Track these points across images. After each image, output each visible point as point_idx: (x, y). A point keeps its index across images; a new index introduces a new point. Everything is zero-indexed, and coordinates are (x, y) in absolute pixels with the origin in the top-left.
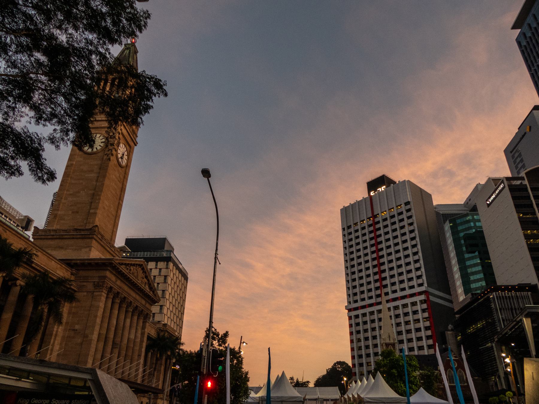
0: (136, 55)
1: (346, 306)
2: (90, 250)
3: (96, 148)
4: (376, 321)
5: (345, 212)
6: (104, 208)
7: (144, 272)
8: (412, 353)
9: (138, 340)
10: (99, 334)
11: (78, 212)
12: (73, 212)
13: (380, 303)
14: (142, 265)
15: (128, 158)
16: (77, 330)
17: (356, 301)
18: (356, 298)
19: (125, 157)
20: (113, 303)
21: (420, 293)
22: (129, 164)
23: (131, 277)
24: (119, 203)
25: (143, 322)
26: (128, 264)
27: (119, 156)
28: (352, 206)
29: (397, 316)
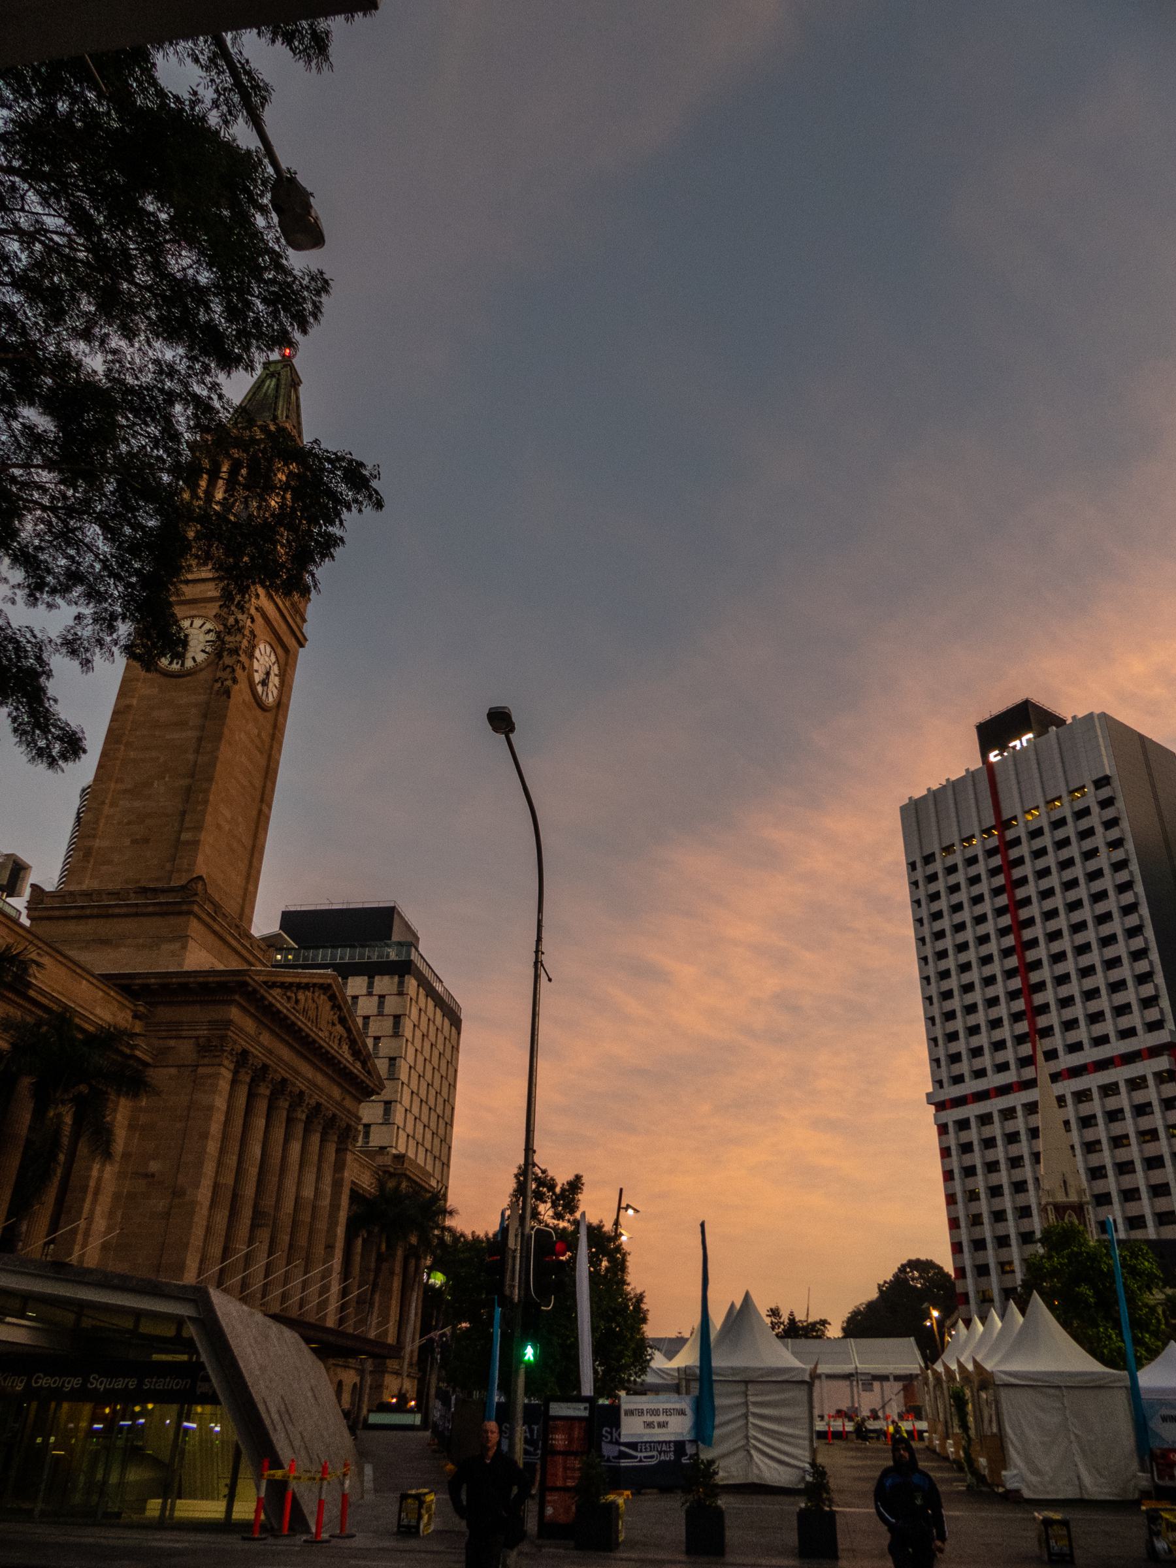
0: (296, 391)
1: (928, 1095)
2: (184, 947)
3: (194, 658)
4: (1023, 1137)
5: (916, 815)
6: (219, 827)
7: (336, 1007)
8: (1138, 1234)
9: (326, 1202)
10: (216, 1186)
11: (146, 841)
12: (134, 842)
13: (1031, 1084)
14: (330, 985)
15: (282, 682)
16: (153, 1175)
17: (958, 1079)
18: (957, 1069)
19: (274, 680)
20: (251, 1096)
21: (1154, 1052)
22: (284, 700)
23: (301, 1022)
24: (260, 811)
25: (338, 1151)
26: (291, 984)
27: (257, 677)
28: (935, 796)
29: (1087, 1122)
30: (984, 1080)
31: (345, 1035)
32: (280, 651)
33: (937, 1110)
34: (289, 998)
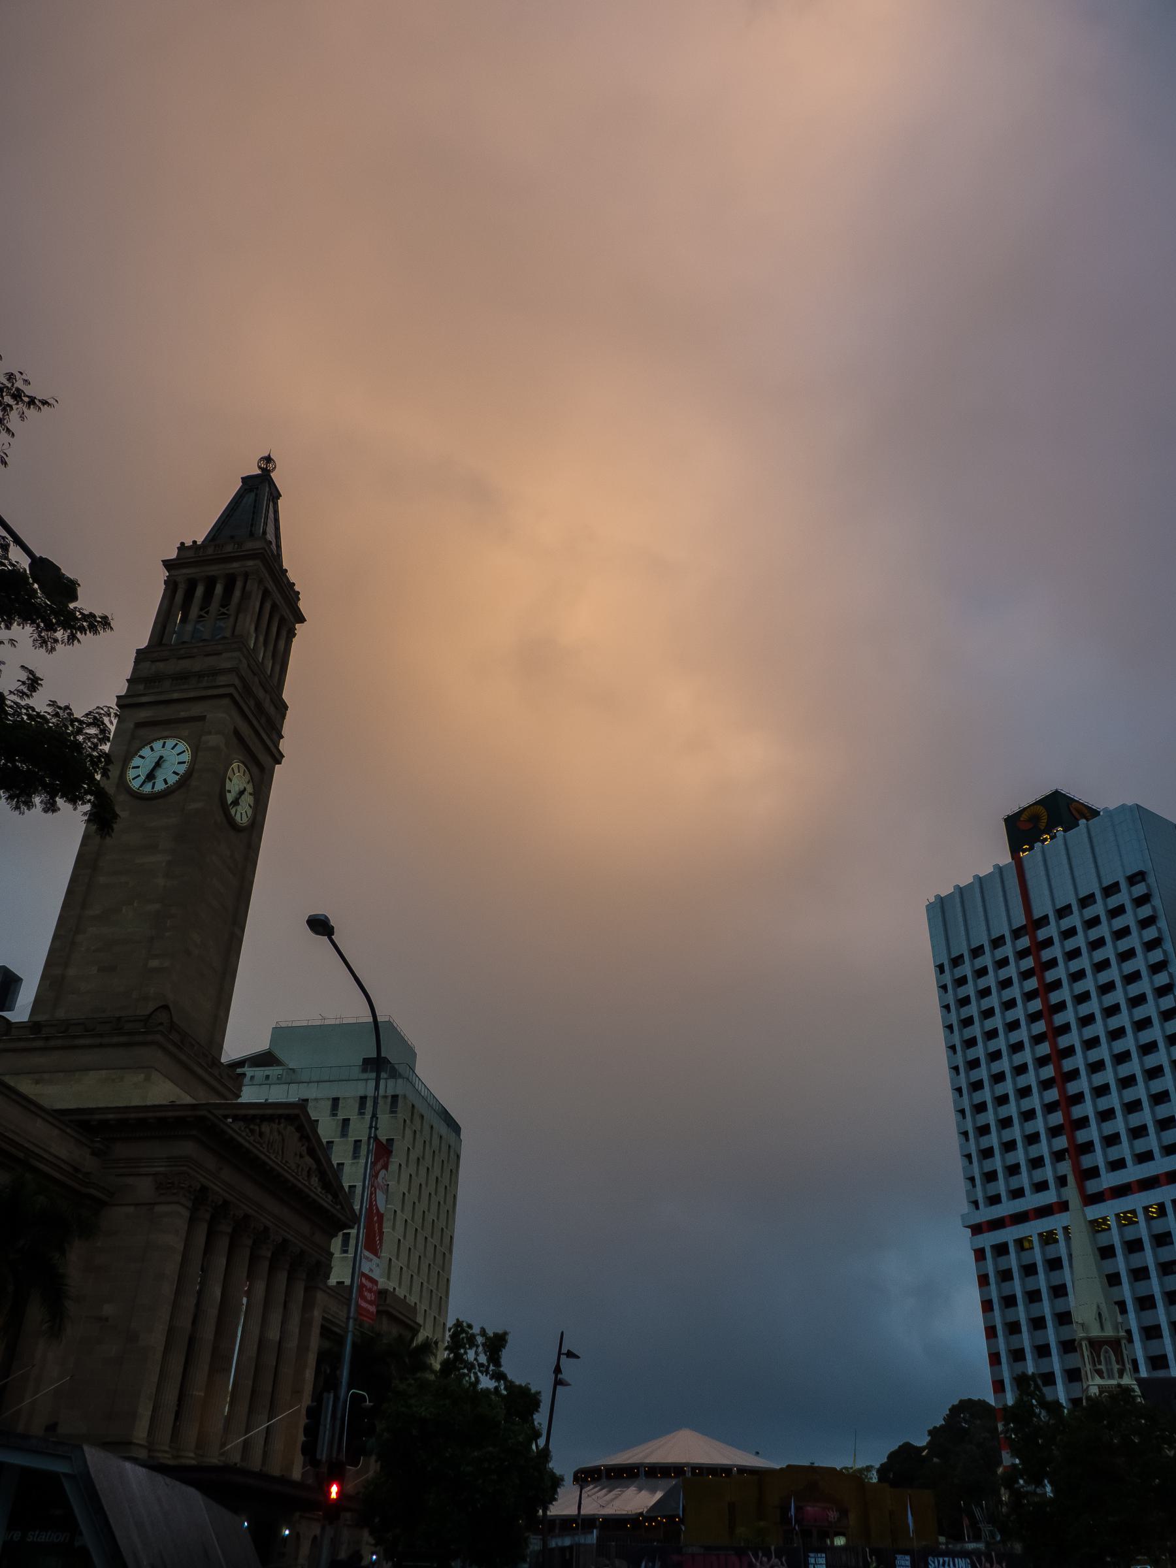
0: (276, 505)
9: (292, 1344)
10: (171, 1331)
14: (297, 1116)
15: (257, 801)
17: (994, 1200)
19: (247, 800)
20: (211, 1235)
25: (306, 1289)
26: (254, 1117)
27: (230, 798)
30: (1021, 1200)
31: (314, 1166)
32: (255, 770)
33: (973, 1234)
34: (252, 1131)
